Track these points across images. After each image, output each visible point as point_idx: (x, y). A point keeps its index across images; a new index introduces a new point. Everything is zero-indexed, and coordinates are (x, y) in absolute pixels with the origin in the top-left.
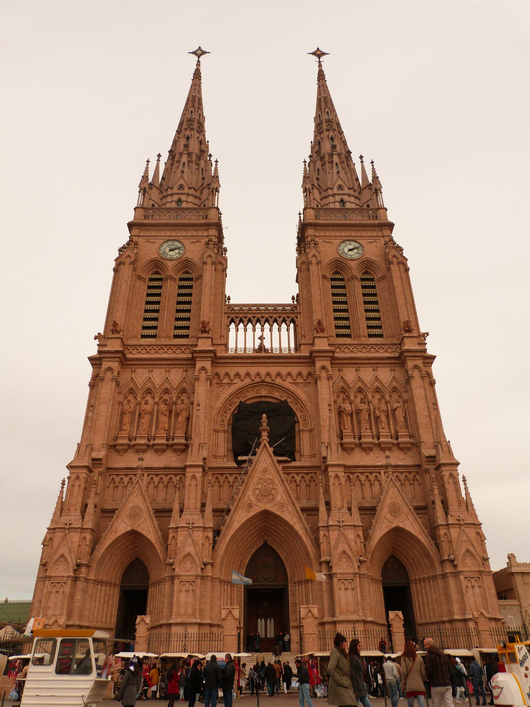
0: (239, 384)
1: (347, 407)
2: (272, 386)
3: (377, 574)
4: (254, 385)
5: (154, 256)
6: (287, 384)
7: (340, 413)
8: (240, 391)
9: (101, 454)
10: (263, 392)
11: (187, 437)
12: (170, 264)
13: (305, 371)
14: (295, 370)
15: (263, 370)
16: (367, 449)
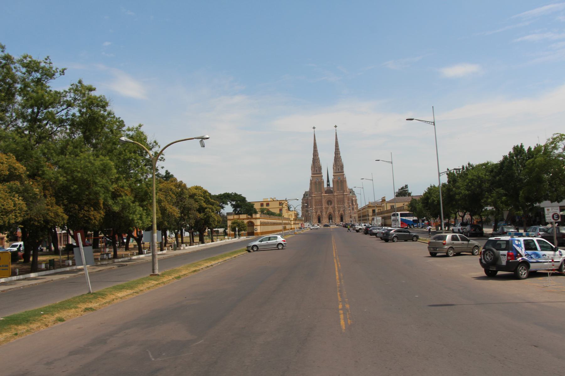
0: (327, 198)
1: (338, 200)
2: (330, 198)
3: (340, 216)
4: (328, 198)
5: (315, 181)
6: (332, 198)
7: (337, 201)
8: (327, 199)
9: (314, 207)
10: (329, 199)
11: (322, 204)
12: (317, 182)
13: (333, 196)
14: (332, 196)
15: (329, 196)
16: (340, 205)
